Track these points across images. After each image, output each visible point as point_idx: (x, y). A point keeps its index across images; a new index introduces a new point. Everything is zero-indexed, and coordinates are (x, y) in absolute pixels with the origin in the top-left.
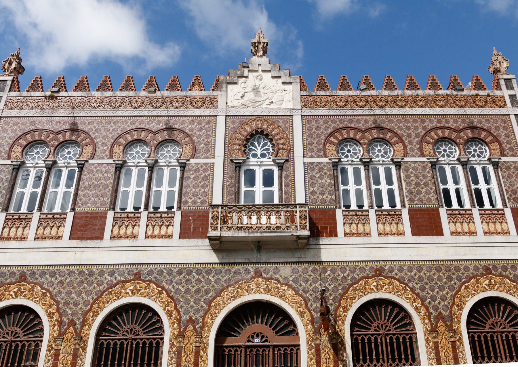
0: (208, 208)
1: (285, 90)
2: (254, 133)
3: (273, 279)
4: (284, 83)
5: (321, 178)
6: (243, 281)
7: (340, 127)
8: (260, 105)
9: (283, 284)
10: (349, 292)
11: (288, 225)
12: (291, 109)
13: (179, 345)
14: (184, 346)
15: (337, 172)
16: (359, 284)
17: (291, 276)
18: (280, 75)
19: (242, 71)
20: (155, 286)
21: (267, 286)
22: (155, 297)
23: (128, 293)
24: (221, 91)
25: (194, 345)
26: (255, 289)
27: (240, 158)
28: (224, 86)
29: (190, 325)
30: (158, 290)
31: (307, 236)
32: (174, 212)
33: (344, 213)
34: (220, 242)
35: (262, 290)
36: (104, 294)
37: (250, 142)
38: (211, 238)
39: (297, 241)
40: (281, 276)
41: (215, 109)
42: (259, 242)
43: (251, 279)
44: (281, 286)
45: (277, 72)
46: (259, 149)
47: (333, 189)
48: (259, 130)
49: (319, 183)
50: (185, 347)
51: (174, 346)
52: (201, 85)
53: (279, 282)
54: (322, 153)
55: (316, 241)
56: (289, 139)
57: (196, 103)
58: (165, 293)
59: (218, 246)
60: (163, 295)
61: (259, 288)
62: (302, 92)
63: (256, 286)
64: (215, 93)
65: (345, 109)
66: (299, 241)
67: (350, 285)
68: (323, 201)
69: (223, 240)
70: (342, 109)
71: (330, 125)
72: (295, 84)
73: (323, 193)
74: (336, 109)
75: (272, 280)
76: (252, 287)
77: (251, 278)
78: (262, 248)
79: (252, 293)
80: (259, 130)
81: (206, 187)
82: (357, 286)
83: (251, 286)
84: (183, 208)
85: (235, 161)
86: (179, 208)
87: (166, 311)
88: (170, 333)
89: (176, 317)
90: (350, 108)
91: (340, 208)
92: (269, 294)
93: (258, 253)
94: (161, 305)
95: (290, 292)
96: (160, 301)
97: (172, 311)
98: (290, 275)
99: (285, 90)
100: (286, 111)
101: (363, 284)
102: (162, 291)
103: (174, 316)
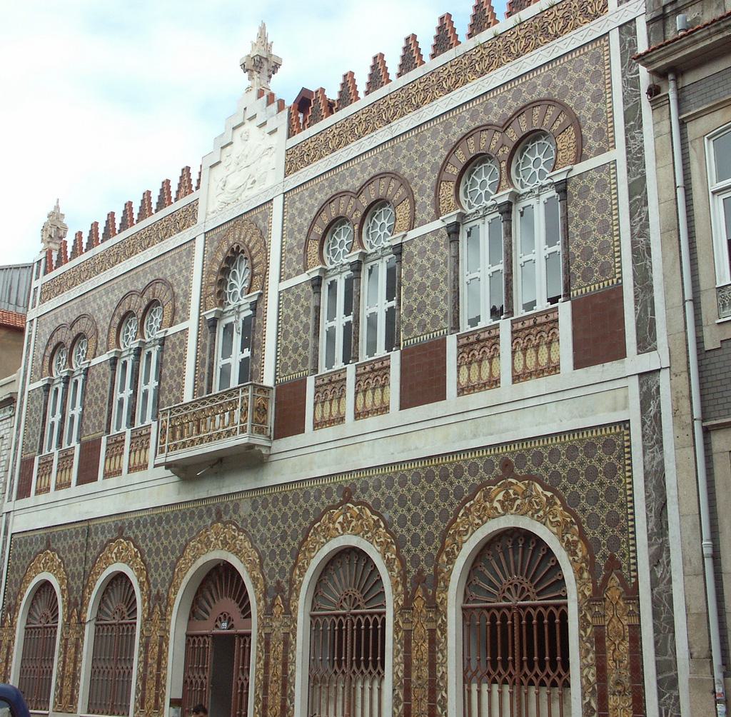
13: (597, 622)
14: (607, 623)
20: (539, 489)
22: (541, 513)
23: (496, 508)
25: (625, 623)
29: (614, 575)
30: (545, 495)
36: (460, 516)
50: (608, 625)
51: (588, 623)
58: (559, 503)
60: (556, 507)
87: (564, 544)
88: (578, 593)
89: (584, 557)
94: (555, 530)
96: (551, 522)
97: (575, 543)
102: (552, 497)
103: (580, 554)
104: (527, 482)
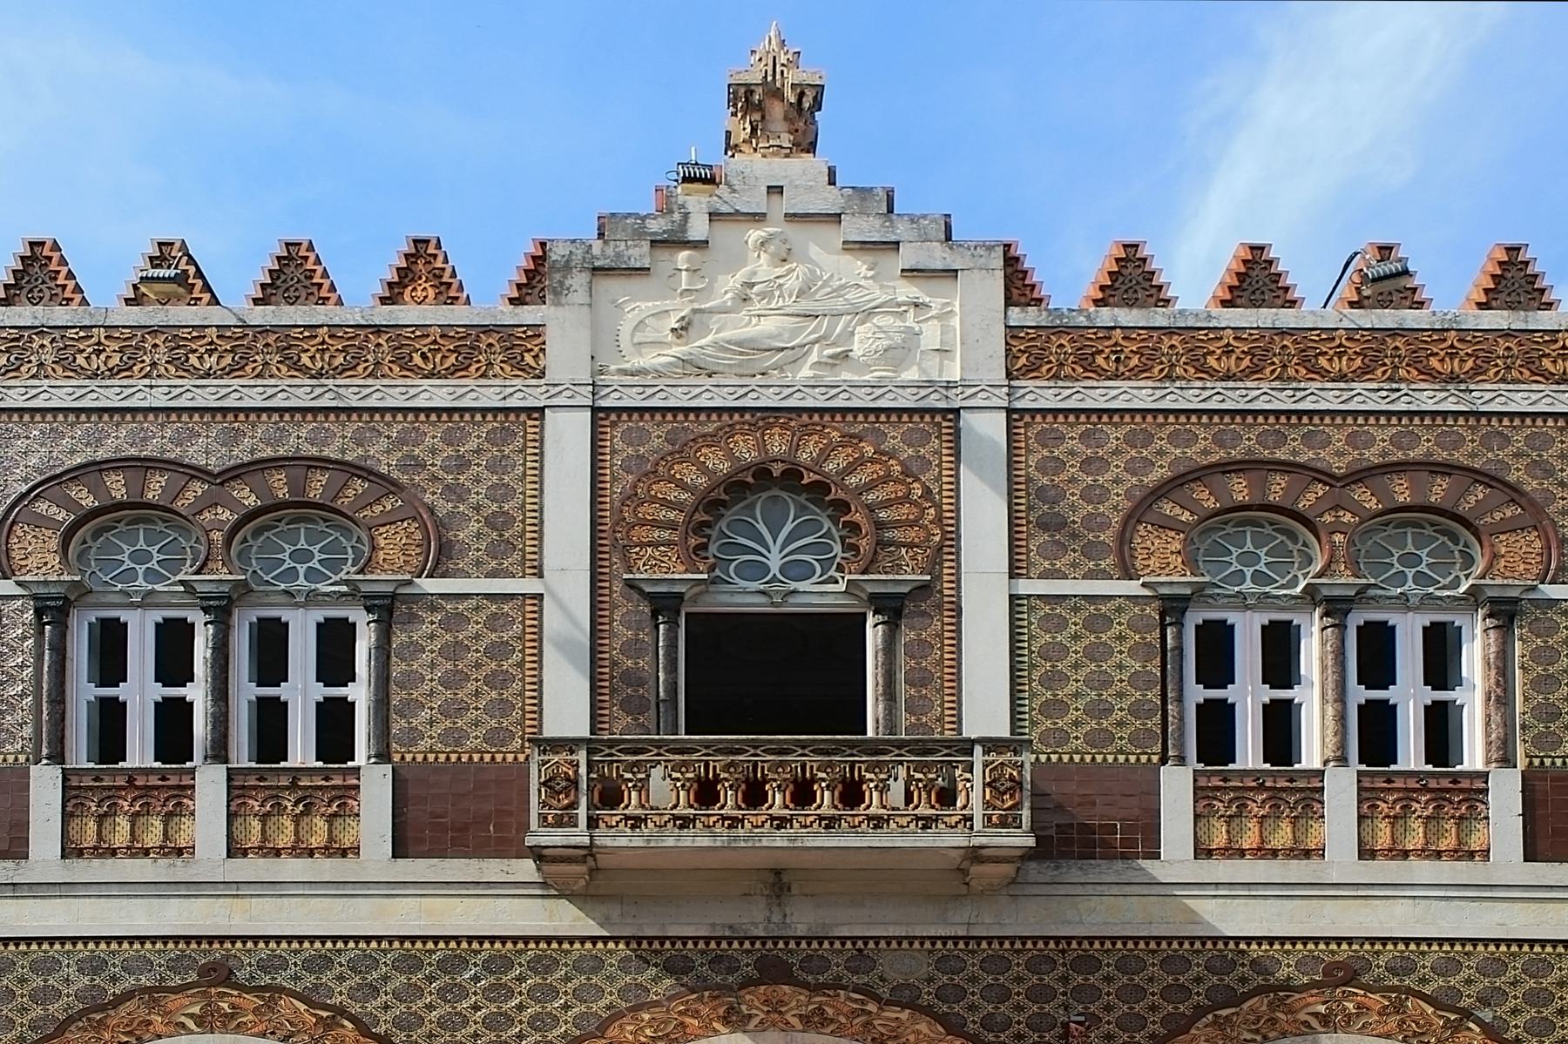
0: (521, 758)
1: (916, 305)
2: (750, 480)
3: (844, 988)
4: (911, 273)
5: (1096, 653)
6: (707, 994)
7: (1213, 458)
8: (779, 367)
9: (889, 1003)
10: (1193, 1031)
11: (924, 810)
12: (949, 386)
15: (1179, 637)
16: (1245, 1006)
17: (930, 980)
18: (893, 238)
19: (677, 217)
21: (819, 1008)
24: (558, 304)
26: (762, 1016)
27: (677, 576)
28: (578, 280)
31: (1018, 853)
32: (358, 768)
33: (1202, 782)
34: (593, 871)
35: (795, 1021)
37: (730, 515)
38: (546, 852)
39: (964, 872)
40: (882, 979)
41: (534, 382)
42: (778, 873)
43: (740, 989)
44: (880, 1008)
45: (877, 222)
46: (775, 549)
47: (1154, 696)
48: (777, 470)
49: (1083, 672)
52: (446, 279)
53: (877, 999)
54: (1107, 563)
55: (1055, 873)
56: (938, 506)
57: (424, 356)
59: (582, 883)
61: (780, 1013)
62: (1015, 312)
63: (766, 1009)
64: (529, 314)
65: (1249, 384)
66: (975, 869)
67: (1200, 1011)
68: (1100, 739)
69: (603, 861)
70: (1231, 384)
71: (1161, 453)
72: (976, 274)
73: (1099, 710)
74: (1199, 384)
75: (842, 992)
76: (746, 1012)
77: (742, 986)
78: (794, 891)
79: (751, 1026)
80: (777, 470)
81: (504, 684)
82: (1237, 1014)
83: (744, 1007)
84: (397, 758)
85: (648, 589)
86: (383, 756)
90: (1276, 384)
91: (1181, 760)
92: (828, 1030)
93: (775, 909)
95: (923, 1027)
98: (926, 976)
99: (916, 305)
100: (923, 392)
101: (1264, 1008)
104: (268, 995)
